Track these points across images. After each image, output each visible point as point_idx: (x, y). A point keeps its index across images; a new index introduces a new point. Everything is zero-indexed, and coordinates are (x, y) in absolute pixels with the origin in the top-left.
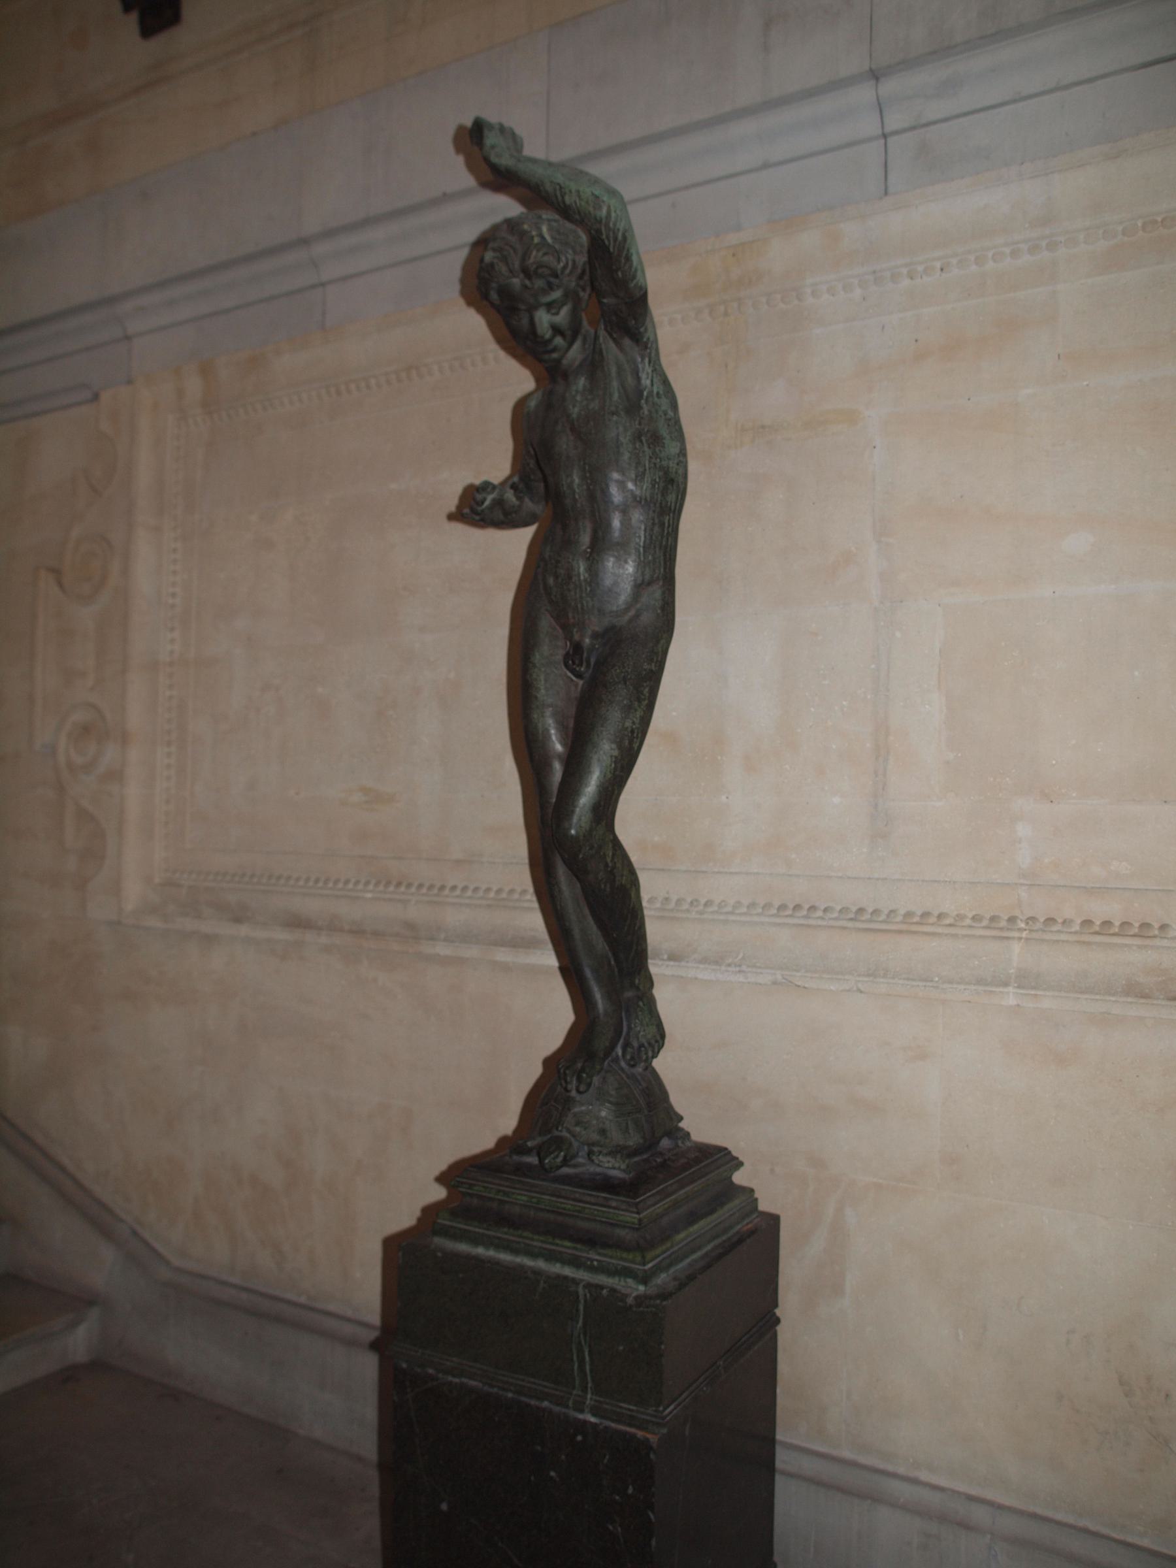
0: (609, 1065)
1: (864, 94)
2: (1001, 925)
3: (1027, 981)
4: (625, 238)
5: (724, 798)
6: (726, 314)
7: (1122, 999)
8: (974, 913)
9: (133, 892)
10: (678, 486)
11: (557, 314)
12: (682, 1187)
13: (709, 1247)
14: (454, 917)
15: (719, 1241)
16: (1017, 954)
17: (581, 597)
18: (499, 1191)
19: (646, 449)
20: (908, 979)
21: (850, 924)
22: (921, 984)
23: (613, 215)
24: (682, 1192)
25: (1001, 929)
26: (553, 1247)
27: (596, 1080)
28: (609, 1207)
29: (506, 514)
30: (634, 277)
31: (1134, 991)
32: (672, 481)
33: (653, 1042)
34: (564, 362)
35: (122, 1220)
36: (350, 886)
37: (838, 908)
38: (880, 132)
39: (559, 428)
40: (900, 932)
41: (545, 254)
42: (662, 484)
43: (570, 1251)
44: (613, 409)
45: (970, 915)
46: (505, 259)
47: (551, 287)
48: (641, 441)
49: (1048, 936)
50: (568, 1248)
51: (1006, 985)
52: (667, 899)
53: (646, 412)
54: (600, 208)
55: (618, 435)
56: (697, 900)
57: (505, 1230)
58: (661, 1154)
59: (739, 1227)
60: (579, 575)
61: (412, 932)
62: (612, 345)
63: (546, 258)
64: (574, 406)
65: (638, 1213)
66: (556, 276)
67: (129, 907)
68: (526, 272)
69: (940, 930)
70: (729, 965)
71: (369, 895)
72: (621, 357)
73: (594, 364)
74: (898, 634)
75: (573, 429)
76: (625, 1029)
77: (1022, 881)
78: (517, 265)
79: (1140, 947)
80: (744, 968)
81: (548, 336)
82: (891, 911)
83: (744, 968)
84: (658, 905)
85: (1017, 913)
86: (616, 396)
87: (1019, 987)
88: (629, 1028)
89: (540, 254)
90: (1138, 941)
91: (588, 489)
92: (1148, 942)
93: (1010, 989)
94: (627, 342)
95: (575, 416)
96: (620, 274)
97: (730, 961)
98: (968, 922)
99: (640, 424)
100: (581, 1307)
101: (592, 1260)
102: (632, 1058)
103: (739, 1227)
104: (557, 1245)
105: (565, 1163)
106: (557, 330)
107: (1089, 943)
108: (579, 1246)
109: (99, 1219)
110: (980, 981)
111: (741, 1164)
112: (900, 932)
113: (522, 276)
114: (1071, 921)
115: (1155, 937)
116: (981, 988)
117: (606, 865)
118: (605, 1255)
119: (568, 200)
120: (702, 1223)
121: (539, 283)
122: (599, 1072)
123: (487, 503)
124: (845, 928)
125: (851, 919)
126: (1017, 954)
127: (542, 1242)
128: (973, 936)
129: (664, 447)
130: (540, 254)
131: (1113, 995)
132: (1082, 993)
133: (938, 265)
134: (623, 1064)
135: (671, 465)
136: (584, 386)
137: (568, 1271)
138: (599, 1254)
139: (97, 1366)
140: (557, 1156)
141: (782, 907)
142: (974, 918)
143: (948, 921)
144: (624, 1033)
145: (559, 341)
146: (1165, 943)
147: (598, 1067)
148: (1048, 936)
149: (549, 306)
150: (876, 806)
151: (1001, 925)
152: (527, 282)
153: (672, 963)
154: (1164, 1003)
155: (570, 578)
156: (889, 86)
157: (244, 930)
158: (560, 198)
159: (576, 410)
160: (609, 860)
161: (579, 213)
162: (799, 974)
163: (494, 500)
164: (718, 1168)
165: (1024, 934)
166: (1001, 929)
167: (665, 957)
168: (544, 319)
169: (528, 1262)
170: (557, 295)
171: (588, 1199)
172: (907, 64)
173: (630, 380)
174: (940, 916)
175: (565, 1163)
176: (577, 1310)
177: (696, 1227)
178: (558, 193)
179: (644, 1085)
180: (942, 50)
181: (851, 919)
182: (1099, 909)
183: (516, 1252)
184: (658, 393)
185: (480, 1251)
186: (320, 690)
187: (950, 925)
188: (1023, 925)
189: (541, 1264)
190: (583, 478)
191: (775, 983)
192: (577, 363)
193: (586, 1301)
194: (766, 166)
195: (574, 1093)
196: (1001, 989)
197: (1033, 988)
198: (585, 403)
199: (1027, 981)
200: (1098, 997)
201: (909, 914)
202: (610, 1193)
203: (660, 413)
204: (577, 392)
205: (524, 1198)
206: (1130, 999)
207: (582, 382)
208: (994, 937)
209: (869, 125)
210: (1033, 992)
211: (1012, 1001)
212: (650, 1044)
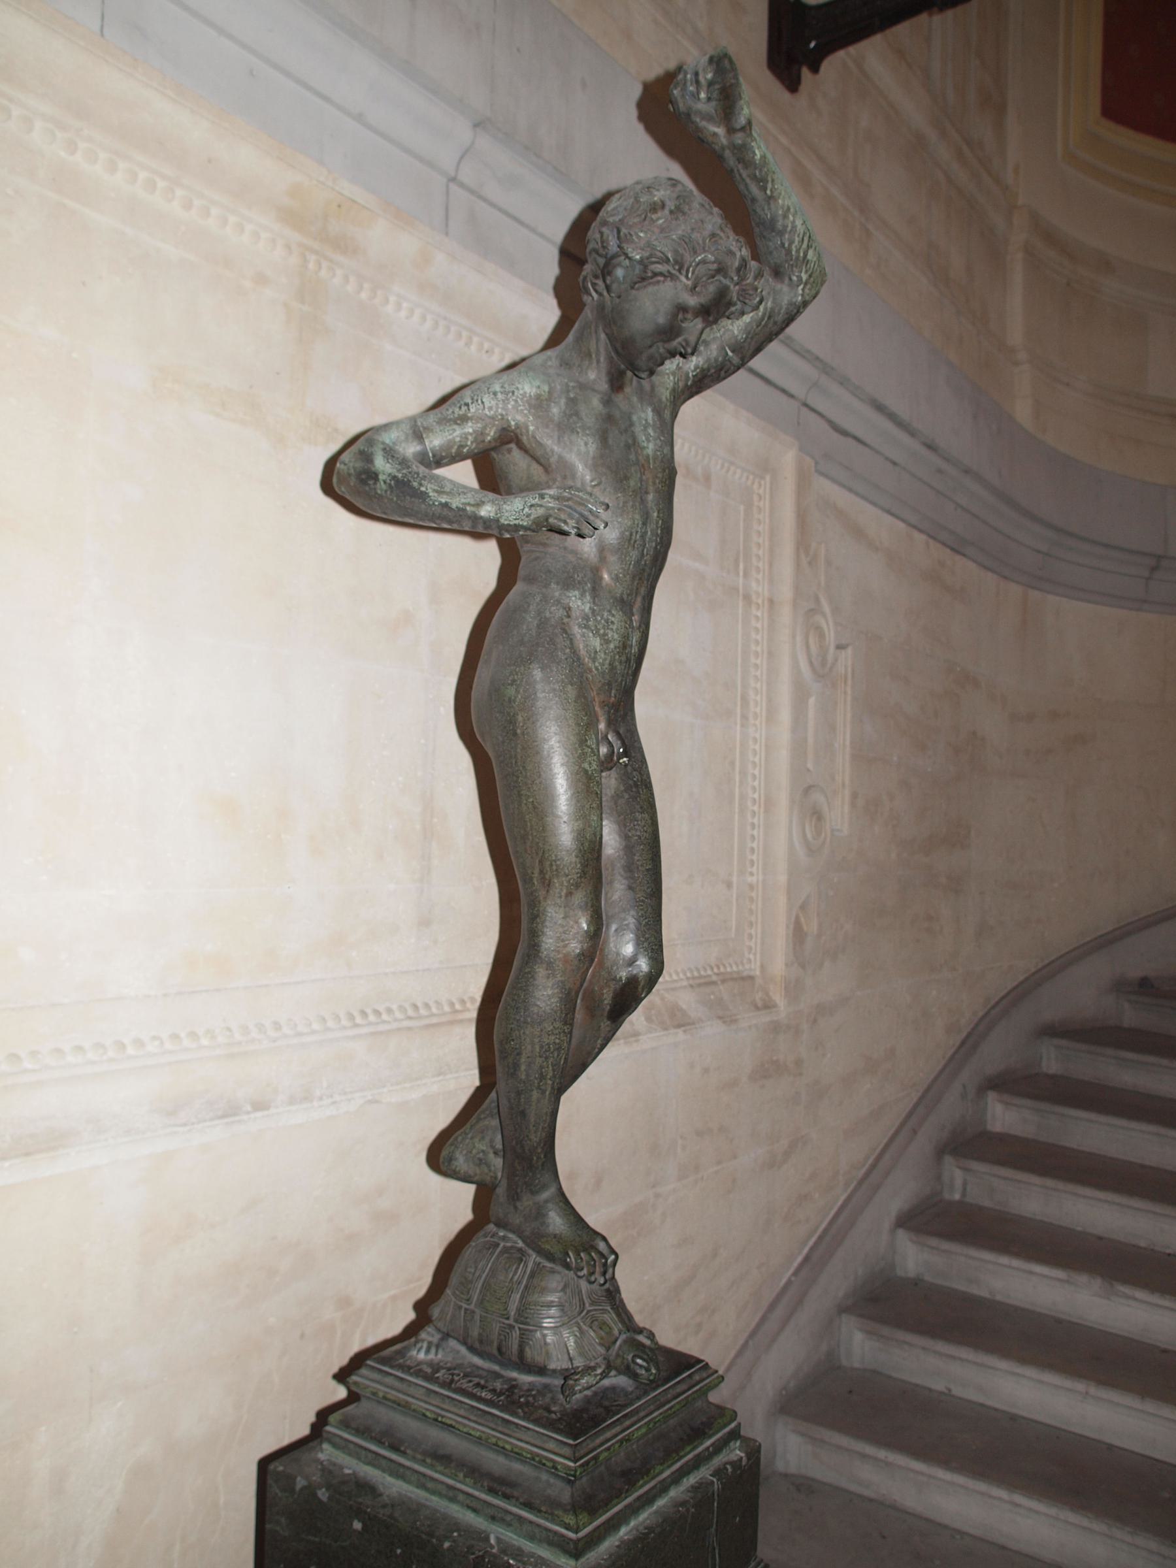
64: (648, 441)
70: (321, 1099)
91: (656, 548)
97: (318, 1093)
101: (708, 1448)
118: (714, 1434)
124: (409, 1029)
127: (669, 1467)
137: (691, 1480)
138: (710, 1437)
153: (259, 1114)
159: (651, 446)
162: (385, 1090)
167: (249, 1108)
169: (661, 1503)
171: (679, 1389)
189: (673, 1493)
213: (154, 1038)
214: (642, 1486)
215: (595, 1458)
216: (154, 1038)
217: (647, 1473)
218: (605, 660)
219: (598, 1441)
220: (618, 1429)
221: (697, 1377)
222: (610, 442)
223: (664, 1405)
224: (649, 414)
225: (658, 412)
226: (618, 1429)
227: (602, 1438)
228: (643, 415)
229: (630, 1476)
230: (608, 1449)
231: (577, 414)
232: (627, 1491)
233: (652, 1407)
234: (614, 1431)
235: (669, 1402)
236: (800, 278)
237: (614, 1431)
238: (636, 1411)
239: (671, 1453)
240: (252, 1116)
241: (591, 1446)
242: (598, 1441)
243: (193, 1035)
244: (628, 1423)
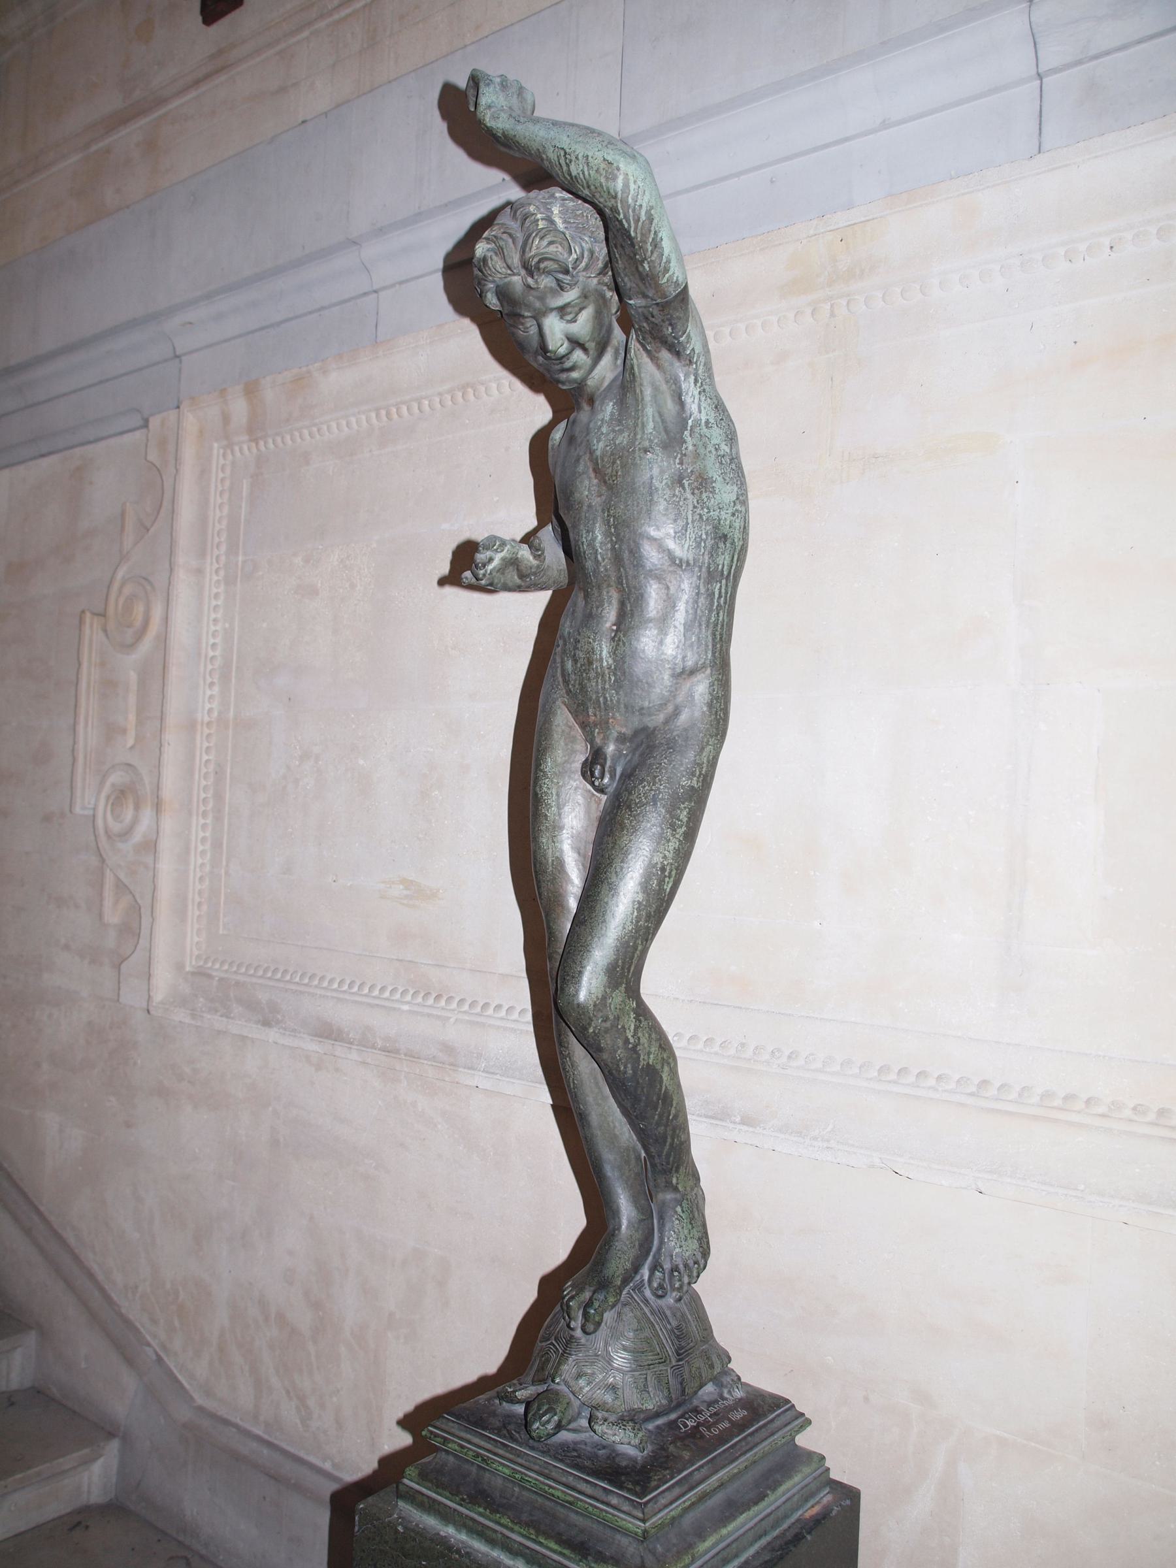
0: (629, 1293)
4: (651, 219)
5: (816, 923)
6: (832, 315)
9: (163, 980)
10: (733, 543)
11: (574, 321)
12: (716, 1472)
13: (752, 1551)
15: (763, 1541)
17: (604, 689)
18: (478, 1455)
19: (688, 495)
23: (632, 186)
24: (715, 1478)
26: (537, 1548)
27: (608, 1316)
28: (608, 1504)
29: (522, 576)
30: (666, 270)
32: (724, 537)
33: (690, 1262)
34: (589, 382)
35: (149, 1345)
36: (387, 994)
37: (957, 1077)
38: (1034, 72)
39: (581, 468)
40: (1035, 1118)
41: (551, 243)
42: (710, 542)
43: (555, 1557)
44: (647, 444)
46: (500, 252)
47: (561, 287)
48: (682, 486)
50: (554, 1551)
52: (743, 1045)
53: (691, 448)
54: (615, 178)
55: (652, 478)
56: (779, 1050)
57: (481, 1510)
58: (696, 1411)
59: (800, 1512)
60: (601, 659)
62: (645, 359)
63: (552, 248)
64: (598, 442)
65: (644, 1521)
66: (567, 272)
67: (158, 997)
68: (530, 269)
70: (815, 1139)
72: (658, 375)
73: (627, 383)
75: (596, 471)
76: (656, 1242)
78: (516, 260)
81: (562, 351)
84: (732, 1052)
86: (650, 426)
88: (662, 1242)
89: (545, 242)
91: (613, 548)
94: (665, 355)
96: (646, 265)
98: (1127, 1113)
99: (681, 463)
102: (661, 1286)
103: (800, 1512)
104: (540, 1544)
105: (559, 1427)
106: (575, 343)
108: (566, 1552)
109: (123, 1340)
111: (809, 1422)
112: (1035, 1118)
113: (523, 272)
117: (627, 1041)
120: (742, 1519)
121: (546, 282)
122: (614, 1306)
123: (496, 563)
124: (962, 1105)
125: (972, 1094)
129: (713, 492)
130: (545, 242)
133: (1107, 242)
134: (648, 1293)
135: (723, 515)
136: (612, 414)
139: (113, 1509)
140: (548, 1421)
141: (884, 1069)
143: (1102, 1109)
144: (654, 1249)
145: (578, 356)
147: (611, 1300)
149: (562, 310)
152: (530, 280)
155: (590, 663)
157: (272, 1035)
158: (565, 168)
159: (601, 445)
160: (629, 1035)
163: (503, 559)
164: (773, 1434)
168: (556, 330)
170: (571, 296)
171: (582, 1486)
173: (670, 406)
175: (559, 1427)
177: (730, 1527)
178: (562, 161)
179: (674, 1323)
181: (972, 1094)
183: (492, 1542)
184: (707, 422)
185: (450, 1531)
186: (361, 762)
187: (1103, 1116)
190: (607, 534)
192: (606, 384)
194: (885, 125)
195: (578, 1333)
198: (611, 436)
201: (1047, 1095)
202: (611, 1482)
203: (710, 448)
205: (507, 1471)
207: (609, 408)
212: (686, 1265)
214: (480, 1514)
215: (445, 1439)
217: (494, 1511)
219: (463, 1434)
220: (489, 1446)
221: (614, 1501)
223: (548, 1477)
226: (489, 1446)
227: (469, 1436)
229: (480, 1496)
230: (462, 1447)
232: (463, 1500)
233: (536, 1467)
234: (482, 1443)
235: (555, 1481)
237: (482, 1443)
238: (519, 1454)
239: (560, 1542)
241: (453, 1430)
242: (463, 1434)
244: (501, 1452)
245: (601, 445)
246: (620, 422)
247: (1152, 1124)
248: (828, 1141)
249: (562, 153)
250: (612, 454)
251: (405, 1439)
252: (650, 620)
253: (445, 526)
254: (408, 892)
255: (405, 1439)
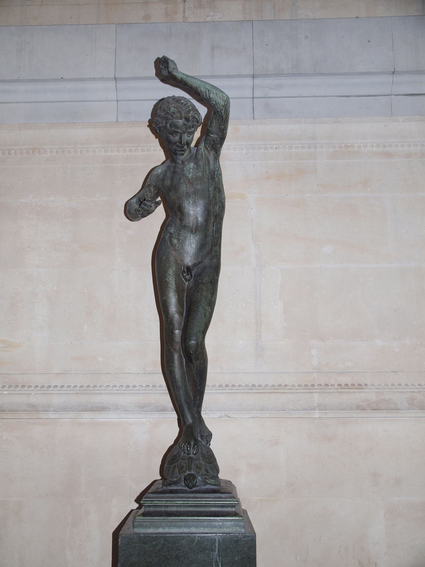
1: (249, 82)
2: (309, 388)
3: (322, 407)
7: (356, 411)
8: (298, 384)
11: (189, 137)
14: (57, 400)
16: (316, 398)
19: (217, 194)
20: (277, 411)
21: (250, 391)
22: (282, 412)
25: (310, 389)
31: (359, 408)
39: (182, 181)
40: (271, 393)
45: (296, 385)
46: (179, 112)
49: (326, 391)
51: (315, 410)
61: (34, 409)
64: (189, 174)
68: (187, 120)
69: (286, 391)
71: (6, 392)
74: (263, 278)
77: (314, 371)
79: (360, 392)
80: (207, 412)
82: (266, 385)
83: (207, 412)
85: (314, 383)
87: (319, 410)
90: (358, 390)
92: (361, 390)
93: (316, 411)
95: (190, 177)
100: (217, 544)
107: (342, 392)
110: (305, 409)
112: (271, 393)
113: (184, 120)
114: (334, 385)
115: (363, 388)
116: (305, 412)
119: (211, 96)
126: (316, 398)
128: (300, 392)
131: (353, 410)
132: (342, 410)
133: (275, 147)
136: (193, 166)
142: (298, 385)
146: (367, 390)
148: (326, 391)
150: (257, 344)
151: (309, 388)
152: (186, 123)
154: (370, 411)
156: (257, 81)
158: (208, 94)
161: (216, 101)
162: (232, 412)
165: (318, 391)
166: (310, 389)
172: (266, 76)
174: (285, 386)
176: (215, 546)
178: (207, 92)
180: (279, 74)
182: (343, 380)
187: (290, 389)
188: (317, 387)
191: (220, 417)
193: (219, 541)
196: (313, 411)
197: (324, 410)
198: (195, 173)
199: (322, 407)
200: (348, 411)
204: (190, 168)
206: (359, 411)
208: (307, 392)
209: (248, 93)
210: (324, 412)
211: (317, 416)
213: (140, 386)
216: (140, 386)
218: (179, 246)
222: (174, 179)
224: (192, 165)
225: (197, 163)
228: (189, 167)
231: (166, 175)
236: (214, 104)
240: (171, 412)
243: (154, 386)
245: (190, 175)
246: (197, 169)
247: (303, 389)
248: (205, 411)
249: (208, 90)
250: (196, 178)
251: (137, 505)
252: (194, 230)
253: (23, 200)
254: (4, 345)
255: (137, 505)
